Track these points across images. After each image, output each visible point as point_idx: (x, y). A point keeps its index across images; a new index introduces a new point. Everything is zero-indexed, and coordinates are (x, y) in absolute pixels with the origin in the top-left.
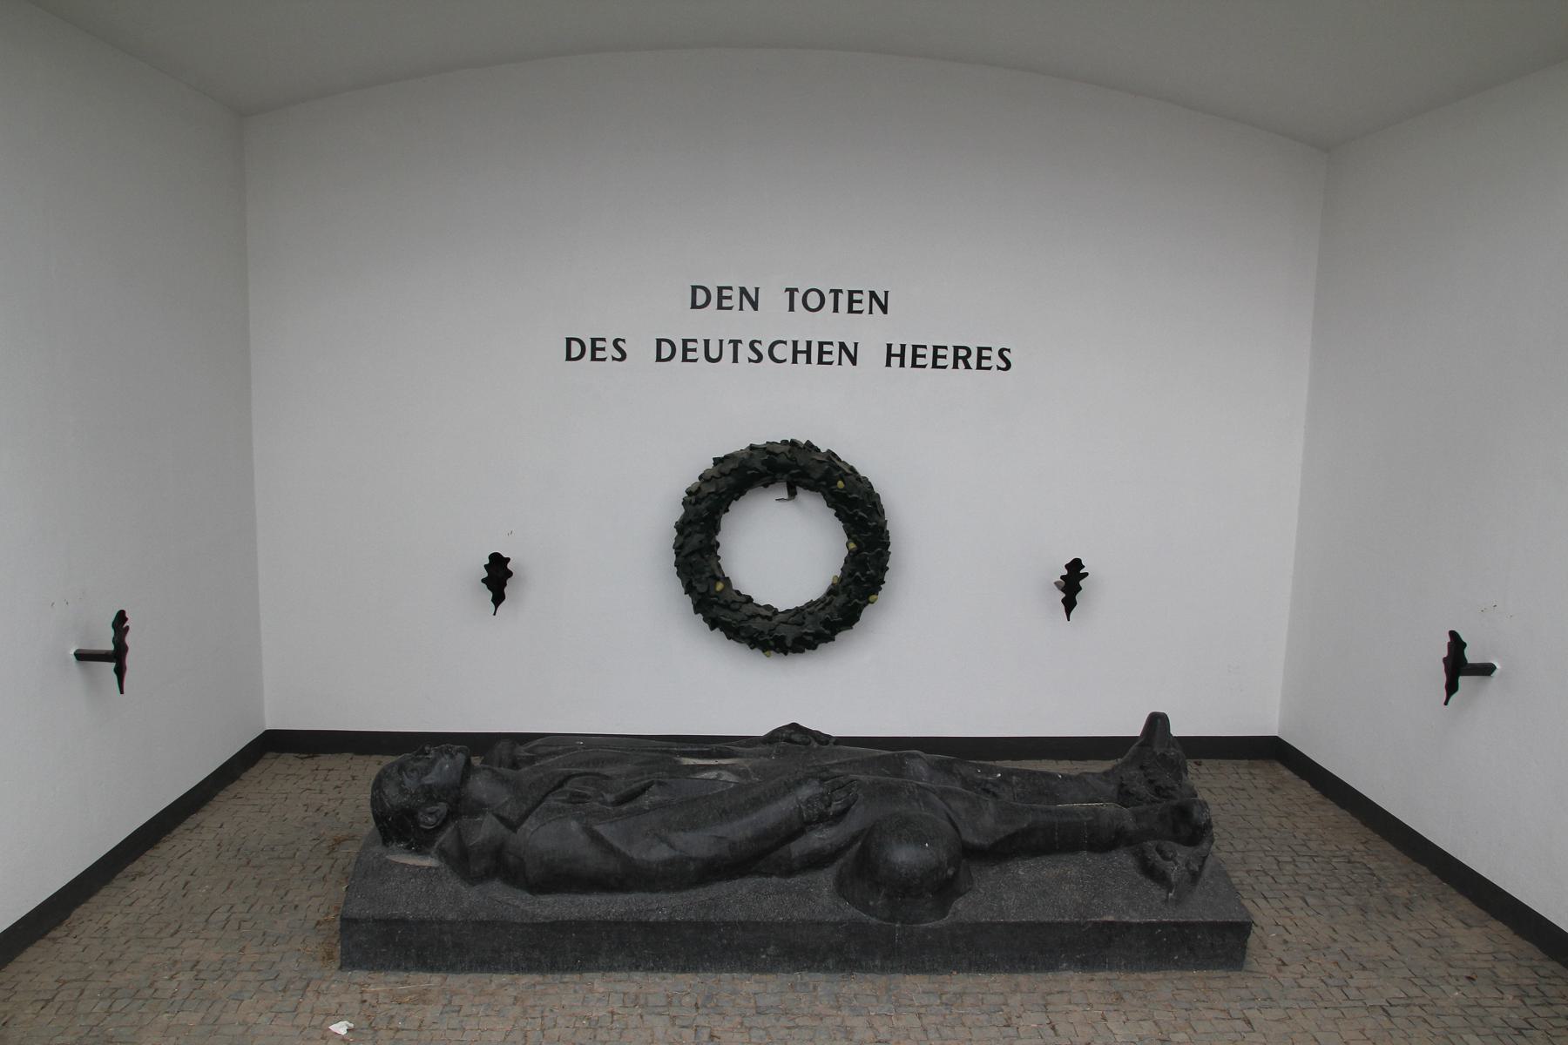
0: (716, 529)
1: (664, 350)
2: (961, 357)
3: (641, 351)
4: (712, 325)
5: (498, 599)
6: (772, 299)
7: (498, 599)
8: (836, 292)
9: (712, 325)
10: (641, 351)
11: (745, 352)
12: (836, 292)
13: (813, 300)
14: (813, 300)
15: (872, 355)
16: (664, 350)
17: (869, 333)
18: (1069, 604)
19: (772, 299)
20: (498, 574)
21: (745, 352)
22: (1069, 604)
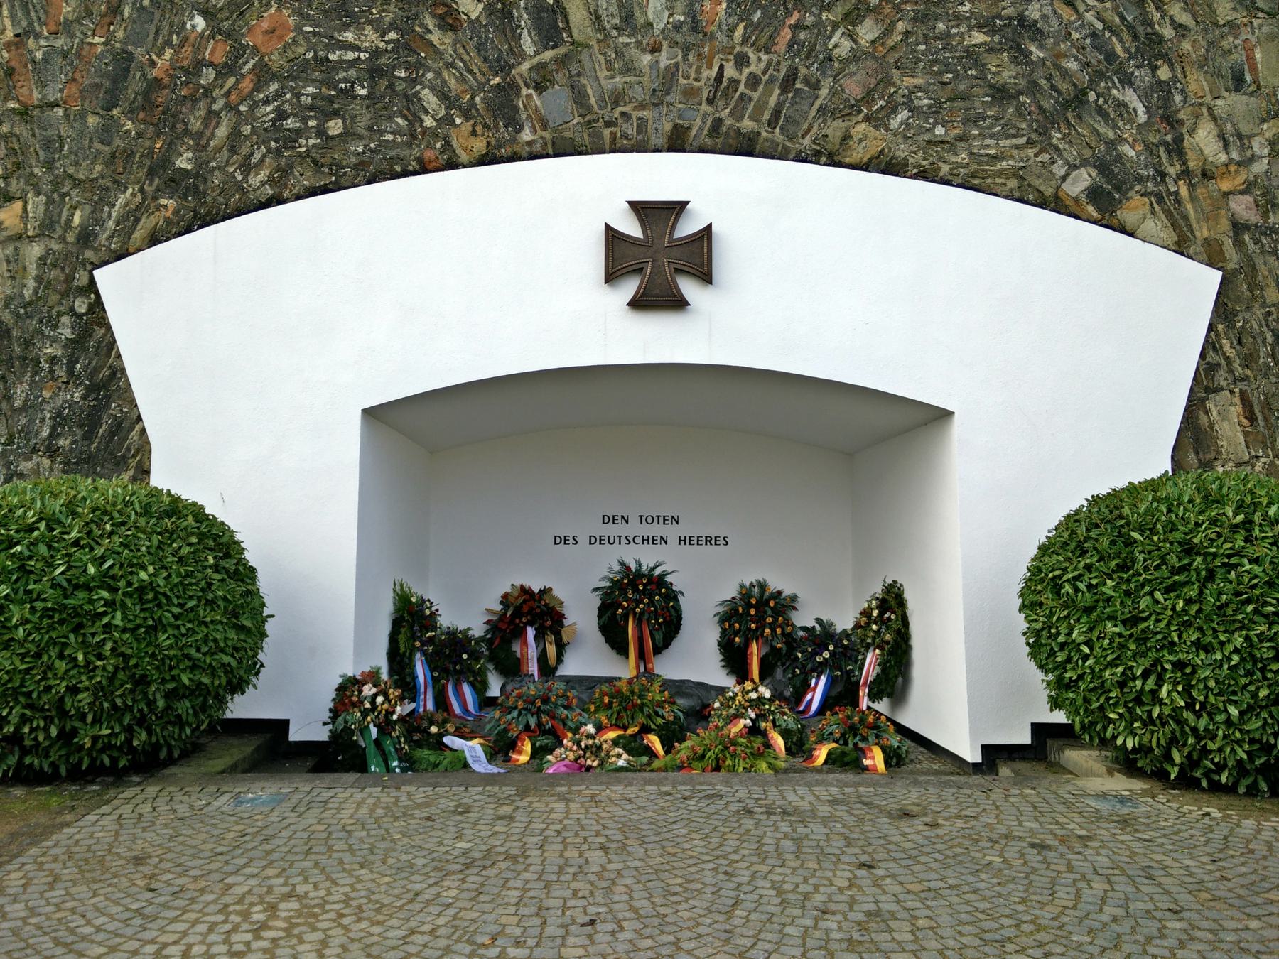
8: (658, 517)
12: (658, 517)
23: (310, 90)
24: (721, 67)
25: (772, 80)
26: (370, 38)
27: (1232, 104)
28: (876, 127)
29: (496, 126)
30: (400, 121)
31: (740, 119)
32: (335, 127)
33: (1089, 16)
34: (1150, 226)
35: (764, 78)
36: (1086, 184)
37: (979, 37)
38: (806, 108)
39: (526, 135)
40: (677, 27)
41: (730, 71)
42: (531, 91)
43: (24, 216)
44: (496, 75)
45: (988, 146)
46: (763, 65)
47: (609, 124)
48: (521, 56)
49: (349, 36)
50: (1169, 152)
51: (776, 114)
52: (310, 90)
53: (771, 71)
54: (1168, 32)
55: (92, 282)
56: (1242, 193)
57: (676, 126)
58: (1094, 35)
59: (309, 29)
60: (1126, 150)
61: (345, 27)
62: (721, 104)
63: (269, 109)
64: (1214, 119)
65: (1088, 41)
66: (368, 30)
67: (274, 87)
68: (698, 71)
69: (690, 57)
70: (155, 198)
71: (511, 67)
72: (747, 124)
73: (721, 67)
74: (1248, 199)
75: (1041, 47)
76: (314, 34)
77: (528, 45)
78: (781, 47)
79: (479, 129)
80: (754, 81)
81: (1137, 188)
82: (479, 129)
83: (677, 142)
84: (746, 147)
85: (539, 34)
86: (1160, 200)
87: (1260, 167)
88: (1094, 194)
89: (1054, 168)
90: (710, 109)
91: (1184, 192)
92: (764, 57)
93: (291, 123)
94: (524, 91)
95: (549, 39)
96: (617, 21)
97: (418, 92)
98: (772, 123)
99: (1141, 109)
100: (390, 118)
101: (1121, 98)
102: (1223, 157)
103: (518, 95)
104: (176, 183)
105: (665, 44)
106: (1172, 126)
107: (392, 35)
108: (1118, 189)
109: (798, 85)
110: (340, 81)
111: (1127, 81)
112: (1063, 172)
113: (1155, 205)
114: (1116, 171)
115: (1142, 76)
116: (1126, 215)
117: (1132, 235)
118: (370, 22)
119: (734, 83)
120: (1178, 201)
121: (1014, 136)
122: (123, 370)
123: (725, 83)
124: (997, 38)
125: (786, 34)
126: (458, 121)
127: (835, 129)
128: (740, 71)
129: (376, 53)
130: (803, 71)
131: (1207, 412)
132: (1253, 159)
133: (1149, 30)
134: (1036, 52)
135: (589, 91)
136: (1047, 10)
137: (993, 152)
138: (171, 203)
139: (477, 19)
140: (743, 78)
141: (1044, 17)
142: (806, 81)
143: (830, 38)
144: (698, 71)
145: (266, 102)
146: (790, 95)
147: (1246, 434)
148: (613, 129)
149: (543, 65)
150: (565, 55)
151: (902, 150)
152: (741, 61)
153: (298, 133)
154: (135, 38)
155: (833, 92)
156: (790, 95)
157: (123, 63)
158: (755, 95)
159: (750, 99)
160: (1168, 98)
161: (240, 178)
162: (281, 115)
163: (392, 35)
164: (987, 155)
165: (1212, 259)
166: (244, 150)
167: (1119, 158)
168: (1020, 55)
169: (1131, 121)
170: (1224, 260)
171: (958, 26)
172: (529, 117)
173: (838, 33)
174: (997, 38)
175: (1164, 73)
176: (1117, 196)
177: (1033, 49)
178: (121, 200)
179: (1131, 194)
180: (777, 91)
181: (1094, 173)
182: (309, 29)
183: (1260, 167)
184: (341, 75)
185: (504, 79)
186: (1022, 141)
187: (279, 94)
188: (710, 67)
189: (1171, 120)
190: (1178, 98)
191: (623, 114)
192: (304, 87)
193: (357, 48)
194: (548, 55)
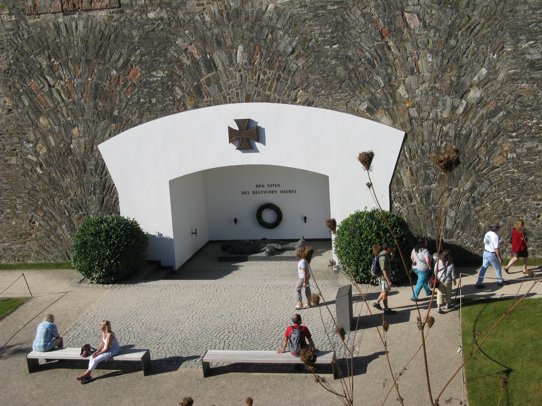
0: (261, 214)
1: (254, 193)
2: (290, 192)
3: (251, 192)
4: (259, 189)
5: (236, 223)
6: (266, 186)
7: (236, 223)
9: (259, 189)
10: (251, 192)
11: (263, 192)
13: (271, 186)
14: (271, 186)
15: (279, 192)
16: (254, 193)
17: (278, 189)
18: (305, 222)
19: (266, 186)
20: (236, 221)
21: (263, 192)
22: (305, 222)
23: (146, 90)
24: (259, 75)
25: (274, 79)
26: (161, 74)
27: (410, 79)
28: (305, 92)
29: (197, 98)
30: (171, 97)
31: (265, 91)
32: (154, 101)
33: (367, 53)
34: (385, 119)
35: (271, 78)
36: (366, 106)
37: (334, 62)
38: (284, 87)
39: (206, 99)
40: (245, 64)
41: (262, 77)
42: (206, 86)
43: (79, 131)
44: (195, 82)
45: (337, 96)
46: (271, 74)
47: (228, 95)
48: (202, 76)
49: (154, 73)
50: (391, 95)
51: (276, 89)
52: (146, 90)
53: (273, 76)
54: (391, 57)
55: (97, 148)
56: (412, 107)
57: (247, 94)
58: (368, 59)
59: (144, 72)
60: (378, 95)
61: (153, 70)
62: (259, 86)
63: (136, 96)
64: (404, 84)
65: (366, 61)
66: (160, 71)
67: (136, 90)
68: (252, 77)
69: (250, 73)
70: (110, 124)
71: (200, 79)
72: (267, 93)
73: (259, 75)
74: (414, 109)
75: (352, 64)
76: (145, 73)
77: (203, 71)
78: (276, 68)
79: (192, 98)
80: (268, 79)
81: (381, 107)
82: (192, 98)
83: (248, 99)
84: (267, 100)
85: (207, 69)
86: (388, 111)
87: (418, 99)
88: (368, 109)
89: (357, 102)
90: (256, 88)
91: (395, 108)
92: (272, 72)
93: (142, 100)
94: (204, 86)
95: (209, 70)
96: (228, 63)
97: (175, 88)
98: (275, 92)
99: (382, 83)
100: (168, 97)
101: (376, 79)
102: (407, 96)
103: (202, 87)
104: (114, 120)
105: (242, 69)
106: (392, 87)
107: (166, 72)
108: (375, 108)
109: (281, 80)
110: (154, 87)
111: (378, 74)
112: (359, 103)
113: (387, 112)
114: (375, 102)
115: (382, 71)
116: (378, 116)
117: (379, 122)
118: (160, 69)
119: (263, 80)
120: (393, 111)
121: (345, 93)
122: (109, 172)
123: (260, 80)
124: (339, 62)
125: (277, 64)
126: (186, 96)
127: (293, 94)
128: (264, 76)
129: (162, 78)
130: (282, 75)
131: (400, 173)
132: (416, 97)
133: (385, 56)
134: (351, 66)
135: (222, 85)
136: (354, 52)
137: (338, 97)
138: (114, 126)
139: (189, 65)
140: (265, 78)
141: (353, 54)
142: (283, 78)
143: (290, 64)
144: (252, 77)
145: (135, 95)
146: (279, 83)
147: (411, 180)
148: (229, 96)
149: (209, 78)
150: (214, 74)
151: (311, 99)
152: (265, 73)
153: (144, 103)
154: (100, 78)
155: (291, 82)
156: (279, 83)
157: (97, 87)
158: (269, 83)
159: (268, 85)
160: (390, 80)
161: (131, 117)
162: (139, 98)
163: (166, 72)
164: (337, 99)
165: (402, 127)
166: (131, 109)
167: (376, 98)
168: (346, 68)
169: (379, 86)
170: (406, 128)
171: (327, 59)
172: (206, 94)
173: (292, 63)
174: (339, 62)
175: (389, 71)
176: (375, 110)
177: (350, 65)
178: (102, 125)
179: (379, 109)
180: (275, 82)
181: (368, 103)
182: (144, 72)
183: (418, 99)
184: (154, 85)
185: (198, 83)
186: (347, 94)
187: (138, 92)
188: (255, 75)
189: (392, 86)
190: (393, 78)
191: (232, 91)
192: (144, 89)
193: (157, 77)
194: (210, 75)
